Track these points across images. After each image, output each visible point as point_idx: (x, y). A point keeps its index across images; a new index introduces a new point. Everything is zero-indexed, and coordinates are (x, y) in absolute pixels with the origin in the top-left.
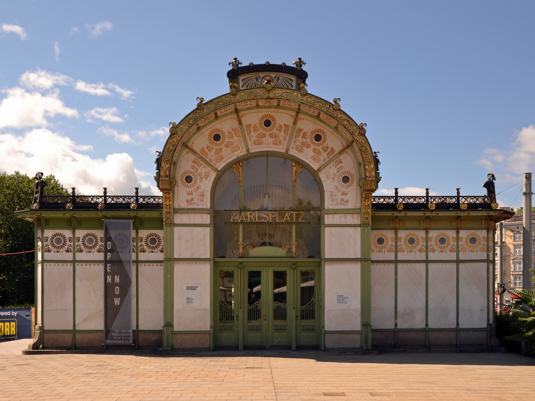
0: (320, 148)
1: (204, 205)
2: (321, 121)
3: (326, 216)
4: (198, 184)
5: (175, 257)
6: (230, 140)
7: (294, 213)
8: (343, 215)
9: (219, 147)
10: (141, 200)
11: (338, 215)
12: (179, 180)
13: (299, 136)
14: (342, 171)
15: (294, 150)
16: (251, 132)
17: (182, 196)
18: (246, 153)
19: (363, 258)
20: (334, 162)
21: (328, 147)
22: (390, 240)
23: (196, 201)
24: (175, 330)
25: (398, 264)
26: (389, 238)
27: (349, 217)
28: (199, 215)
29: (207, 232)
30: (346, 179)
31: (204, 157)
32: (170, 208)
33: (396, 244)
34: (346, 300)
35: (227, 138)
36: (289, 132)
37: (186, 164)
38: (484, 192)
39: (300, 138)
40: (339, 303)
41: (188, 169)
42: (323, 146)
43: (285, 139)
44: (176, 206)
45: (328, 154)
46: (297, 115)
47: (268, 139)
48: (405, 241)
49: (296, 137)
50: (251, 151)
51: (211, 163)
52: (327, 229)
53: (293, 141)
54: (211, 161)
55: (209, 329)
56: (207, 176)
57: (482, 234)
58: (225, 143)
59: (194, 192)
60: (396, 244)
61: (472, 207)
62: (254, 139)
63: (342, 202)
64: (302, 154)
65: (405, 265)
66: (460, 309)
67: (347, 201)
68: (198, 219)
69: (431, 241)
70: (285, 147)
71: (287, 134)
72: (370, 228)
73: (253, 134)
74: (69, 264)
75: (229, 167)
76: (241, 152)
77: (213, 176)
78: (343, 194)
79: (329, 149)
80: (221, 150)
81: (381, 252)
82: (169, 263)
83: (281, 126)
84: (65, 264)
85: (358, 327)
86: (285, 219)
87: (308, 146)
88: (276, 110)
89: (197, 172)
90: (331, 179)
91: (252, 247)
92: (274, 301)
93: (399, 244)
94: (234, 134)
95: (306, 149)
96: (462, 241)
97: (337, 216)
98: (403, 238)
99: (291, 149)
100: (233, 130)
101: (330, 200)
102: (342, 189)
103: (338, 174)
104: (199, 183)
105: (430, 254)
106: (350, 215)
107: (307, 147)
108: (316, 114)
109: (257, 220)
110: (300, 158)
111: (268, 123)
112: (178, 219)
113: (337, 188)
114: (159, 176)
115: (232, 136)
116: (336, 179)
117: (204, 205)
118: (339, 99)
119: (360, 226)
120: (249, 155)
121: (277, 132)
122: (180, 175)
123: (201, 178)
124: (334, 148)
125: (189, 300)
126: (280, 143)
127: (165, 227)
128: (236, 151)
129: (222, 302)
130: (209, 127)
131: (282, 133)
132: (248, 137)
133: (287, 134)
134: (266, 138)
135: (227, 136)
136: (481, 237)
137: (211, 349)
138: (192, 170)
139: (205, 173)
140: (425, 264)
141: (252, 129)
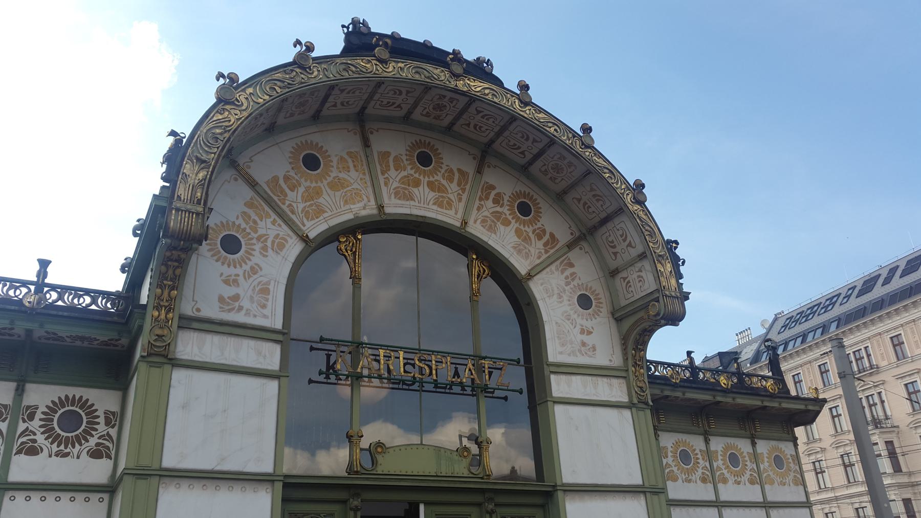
0: (529, 230)
1: (265, 316)
3: (553, 377)
5: (169, 462)
8: (589, 378)
9: (314, 185)
11: (579, 377)
13: (487, 199)
14: (575, 283)
17: (209, 283)
20: (559, 262)
21: (544, 231)
23: (246, 304)
27: (602, 382)
28: (252, 343)
30: (585, 302)
31: (276, 198)
32: (169, 310)
36: (468, 187)
39: (489, 203)
42: (536, 227)
43: (460, 200)
44: (187, 309)
45: (545, 245)
47: (423, 192)
49: (481, 199)
50: (388, 210)
51: (293, 217)
52: (559, 410)
53: (476, 207)
54: (293, 212)
56: (280, 247)
59: (241, 279)
62: (395, 185)
67: (594, 348)
68: (247, 353)
70: (460, 215)
71: (464, 190)
73: (392, 173)
75: (332, 237)
76: (364, 208)
77: (295, 248)
78: (582, 332)
79: (547, 236)
82: (142, 483)
83: (451, 171)
87: (507, 223)
90: (555, 296)
94: (351, 165)
95: (502, 228)
96: (763, 462)
97: (577, 380)
99: (471, 222)
102: (579, 321)
103: (567, 288)
104: (257, 258)
106: (605, 380)
107: (503, 224)
110: (491, 243)
112: (189, 346)
116: (565, 298)
117: (265, 316)
119: (630, 406)
121: (444, 182)
123: (265, 248)
124: (557, 236)
126: (450, 205)
128: (354, 204)
132: (381, 179)
133: (464, 190)
134: (421, 188)
135: (335, 164)
136: (789, 456)
138: (240, 221)
139: (277, 236)
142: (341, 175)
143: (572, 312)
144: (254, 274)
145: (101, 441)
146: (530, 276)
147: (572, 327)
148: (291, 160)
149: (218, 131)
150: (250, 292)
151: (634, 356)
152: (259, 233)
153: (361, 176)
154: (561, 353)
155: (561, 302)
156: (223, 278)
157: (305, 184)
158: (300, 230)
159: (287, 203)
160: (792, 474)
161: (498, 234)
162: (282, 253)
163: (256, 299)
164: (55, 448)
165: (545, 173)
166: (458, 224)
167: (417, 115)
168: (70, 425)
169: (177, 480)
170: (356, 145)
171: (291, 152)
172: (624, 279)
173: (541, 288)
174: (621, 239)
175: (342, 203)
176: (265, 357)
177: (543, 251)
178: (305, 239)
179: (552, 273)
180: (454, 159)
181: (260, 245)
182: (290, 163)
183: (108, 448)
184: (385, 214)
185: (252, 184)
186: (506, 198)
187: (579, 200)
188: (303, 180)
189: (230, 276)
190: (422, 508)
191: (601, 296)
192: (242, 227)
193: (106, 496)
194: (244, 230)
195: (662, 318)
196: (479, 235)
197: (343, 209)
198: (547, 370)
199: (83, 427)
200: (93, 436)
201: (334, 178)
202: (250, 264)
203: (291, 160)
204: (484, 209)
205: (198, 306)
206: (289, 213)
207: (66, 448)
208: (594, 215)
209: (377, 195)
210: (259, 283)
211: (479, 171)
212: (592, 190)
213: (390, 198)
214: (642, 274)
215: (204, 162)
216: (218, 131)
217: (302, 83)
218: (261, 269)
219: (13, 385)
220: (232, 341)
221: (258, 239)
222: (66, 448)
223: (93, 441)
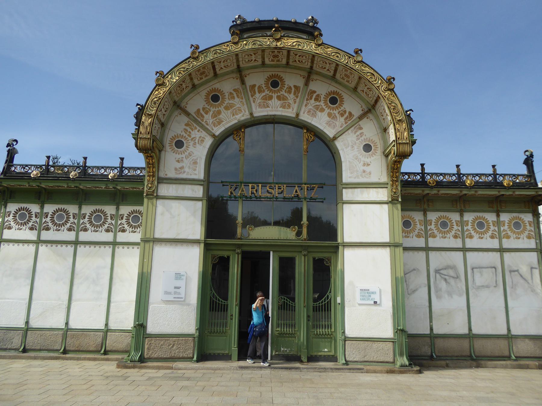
0: (336, 112)
1: (196, 174)
2: (337, 82)
3: (344, 190)
4: (190, 150)
5: (157, 236)
7: (306, 186)
9: (217, 109)
10: (126, 172)
11: (359, 189)
12: (167, 145)
13: (311, 98)
14: (362, 138)
16: (255, 93)
17: (171, 163)
18: (249, 117)
19: (392, 242)
21: (345, 112)
22: (418, 223)
23: (187, 169)
25: (430, 252)
26: (417, 221)
28: (190, 186)
29: (199, 208)
30: (367, 148)
31: (199, 119)
33: (426, 228)
36: (300, 94)
37: (177, 127)
38: (524, 170)
39: (313, 101)
40: (364, 299)
41: (179, 132)
42: (340, 110)
43: (295, 102)
44: (162, 175)
46: (309, 76)
48: (436, 225)
51: (208, 127)
53: (304, 105)
54: (207, 124)
56: (202, 141)
57: (528, 217)
58: (224, 105)
59: (184, 159)
60: (426, 228)
61: (516, 186)
62: (259, 101)
64: (314, 118)
65: (438, 253)
66: (509, 309)
67: (370, 173)
69: (467, 225)
70: (295, 111)
72: (399, 206)
73: (257, 95)
74: (31, 245)
76: (243, 116)
77: (209, 141)
78: (364, 165)
79: (347, 114)
80: (219, 113)
81: (408, 237)
83: (290, 88)
84: (26, 245)
87: (322, 110)
89: (190, 136)
90: (350, 147)
91: (253, 227)
93: (429, 228)
94: (235, 95)
95: (319, 114)
98: (434, 221)
100: (235, 90)
102: (363, 159)
103: (357, 142)
104: (191, 149)
105: (468, 241)
106: (375, 189)
108: (331, 74)
110: (313, 123)
111: (275, 84)
112: (164, 190)
114: (138, 133)
115: (234, 98)
116: (356, 147)
117: (196, 174)
118: (361, 50)
121: (286, 95)
122: (169, 139)
123: (195, 144)
124: (353, 113)
126: (289, 106)
127: (146, 200)
128: (237, 115)
130: (206, 86)
131: (292, 95)
132: (251, 99)
133: (297, 97)
134: (273, 100)
135: (227, 97)
137: (195, 358)
138: (183, 133)
139: (200, 137)
140: (462, 253)
142: (230, 102)
143: (359, 155)
144: (190, 156)
146: (335, 138)
147: (358, 163)
149: (156, 99)
150: (188, 165)
151: (392, 177)
153: (241, 100)
154: (350, 177)
156: (177, 160)
157: (212, 110)
158: (211, 132)
159: (205, 120)
160: (527, 233)
161: (317, 117)
162: (203, 145)
163: (191, 167)
164: (131, 229)
166: (294, 116)
167: (267, 61)
168: (135, 220)
169: (160, 243)
170: (237, 84)
173: (342, 143)
176: (196, 192)
177: (344, 123)
178: (213, 136)
179: (349, 134)
180: (292, 80)
181: (193, 142)
185: (188, 114)
186: (322, 97)
188: (212, 108)
190: (271, 253)
191: (378, 143)
194: (185, 137)
196: (306, 120)
197: (232, 118)
198: (340, 187)
202: (188, 152)
204: (309, 104)
208: (372, 99)
211: (307, 84)
212: (366, 86)
213: (256, 109)
215: (151, 115)
216: (156, 99)
219: (115, 207)
220: (181, 187)
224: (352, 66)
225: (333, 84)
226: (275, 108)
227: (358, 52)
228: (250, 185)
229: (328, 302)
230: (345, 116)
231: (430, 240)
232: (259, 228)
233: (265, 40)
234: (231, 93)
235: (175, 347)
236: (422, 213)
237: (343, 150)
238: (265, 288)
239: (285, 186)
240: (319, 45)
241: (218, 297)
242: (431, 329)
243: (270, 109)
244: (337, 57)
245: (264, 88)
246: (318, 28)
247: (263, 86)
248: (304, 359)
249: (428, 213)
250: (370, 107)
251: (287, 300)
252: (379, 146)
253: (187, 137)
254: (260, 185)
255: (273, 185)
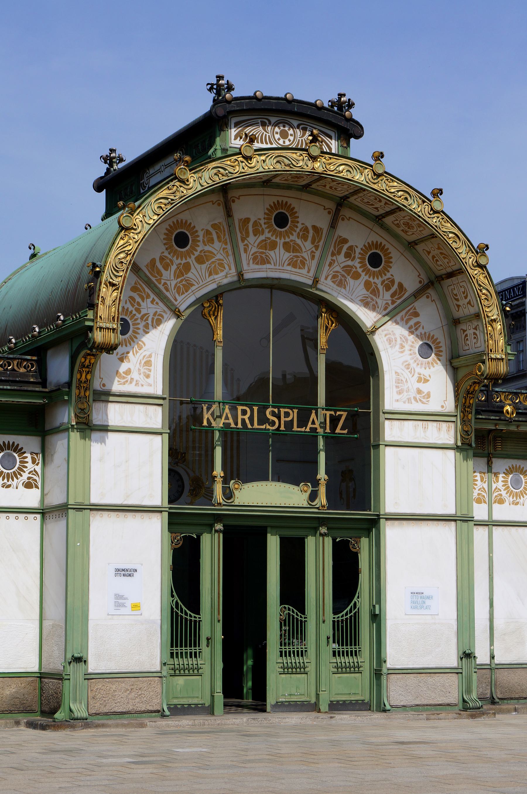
0: (378, 281)
2: (383, 226)
5: (95, 499)
6: (207, 248)
8: (420, 423)
9: (184, 261)
13: (339, 253)
15: (329, 281)
16: (248, 236)
19: (459, 514)
20: (403, 313)
21: (393, 282)
23: (135, 375)
24: (90, 671)
28: (142, 407)
31: (153, 279)
34: (428, 602)
35: (200, 244)
36: (321, 244)
39: (341, 258)
40: (415, 608)
42: (385, 278)
43: (313, 257)
45: (392, 296)
46: (338, 211)
47: (280, 254)
49: (333, 254)
50: (247, 276)
51: (168, 294)
53: (327, 263)
54: (167, 290)
55: (158, 669)
58: (197, 254)
62: (254, 250)
63: (418, 396)
64: (343, 290)
65: (506, 529)
67: (428, 395)
70: (312, 274)
71: (317, 247)
73: (252, 239)
78: (419, 380)
79: (396, 286)
80: (187, 268)
83: (306, 229)
85: (453, 661)
86: (310, 425)
87: (356, 276)
88: (298, 194)
89: (138, 311)
92: (281, 604)
94: (215, 236)
99: (322, 279)
101: (395, 390)
102: (418, 370)
106: (435, 424)
109: (256, 426)
111: (281, 221)
113: (408, 366)
115: (211, 241)
116: (407, 347)
120: (243, 284)
121: (299, 241)
124: (405, 285)
125: (119, 600)
128: (217, 273)
129: (177, 607)
131: (308, 245)
133: (317, 247)
135: (201, 238)
138: (128, 305)
139: (155, 314)
141: (251, 230)
145: (30, 475)
147: (410, 376)
148: (165, 242)
149: (122, 255)
152: (142, 313)
153: (224, 246)
155: (402, 352)
158: (173, 305)
159: (163, 282)
161: (348, 288)
163: (142, 370)
165: (398, 225)
166: (310, 282)
171: (165, 234)
172: (464, 331)
174: (463, 295)
175: (207, 275)
177: (390, 302)
182: (165, 244)
183: (36, 481)
184: (244, 280)
186: (358, 251)
187: (429, 253)
189: (123, 354)
192: (130, 310)
193: (39, 516)
195: (485, 378)
197: (208, 280)
198: (382, 416)
199: (17, 466)
200: (25, 472)
201: (201, 252)
203: (165, 242)
204: (336, 264)
205: (103, 382)
206: (164, 291)
207: (8, 481)
208: (441, 268)
209: (238, 262)
210: (144, 356)
211: (333, 225)
214: (477, 332)
216: (122, 255)
217: (182, 197)
218: (145, 345)
221: (142, 318)
222: (8, 481)
223: (25, 476)
224: (427, 219)
225: (377, 229)
226: (279, 267)
227: (438, 193)
228: (240, 408)
229: (355, 614)
230: (393, 289)
231: (496, 507)
232: (250, 485)
233: (294, 156)
234: (208, 232)
235: (133, 694)
236: (485, 460)
237: (386, 350)
238: (264, 594)
239: (296, 411)
240: (379, 175)
241: (184, 608)
242: (492, 657)
243: (272, 266)
244: (406, 199)
245: (264, 226)
246: (357, 123)
247: (262, 222)
248: (324, 707)
249: (494, 460)
250: (433, 278)
251: (293, 612)
252: (443, 349)
253: (134, 312)
254: (256, 409)
255: (276, 410)
